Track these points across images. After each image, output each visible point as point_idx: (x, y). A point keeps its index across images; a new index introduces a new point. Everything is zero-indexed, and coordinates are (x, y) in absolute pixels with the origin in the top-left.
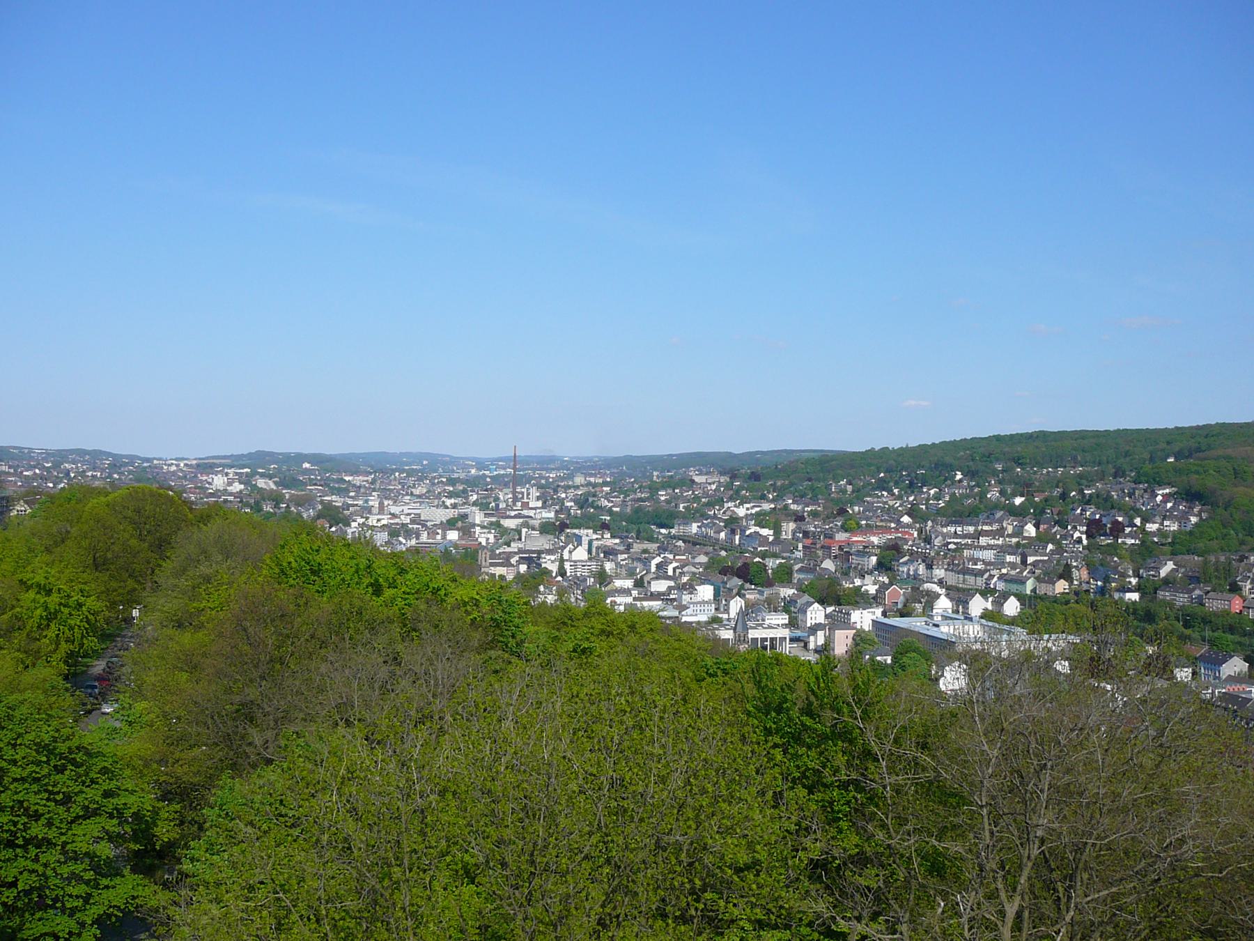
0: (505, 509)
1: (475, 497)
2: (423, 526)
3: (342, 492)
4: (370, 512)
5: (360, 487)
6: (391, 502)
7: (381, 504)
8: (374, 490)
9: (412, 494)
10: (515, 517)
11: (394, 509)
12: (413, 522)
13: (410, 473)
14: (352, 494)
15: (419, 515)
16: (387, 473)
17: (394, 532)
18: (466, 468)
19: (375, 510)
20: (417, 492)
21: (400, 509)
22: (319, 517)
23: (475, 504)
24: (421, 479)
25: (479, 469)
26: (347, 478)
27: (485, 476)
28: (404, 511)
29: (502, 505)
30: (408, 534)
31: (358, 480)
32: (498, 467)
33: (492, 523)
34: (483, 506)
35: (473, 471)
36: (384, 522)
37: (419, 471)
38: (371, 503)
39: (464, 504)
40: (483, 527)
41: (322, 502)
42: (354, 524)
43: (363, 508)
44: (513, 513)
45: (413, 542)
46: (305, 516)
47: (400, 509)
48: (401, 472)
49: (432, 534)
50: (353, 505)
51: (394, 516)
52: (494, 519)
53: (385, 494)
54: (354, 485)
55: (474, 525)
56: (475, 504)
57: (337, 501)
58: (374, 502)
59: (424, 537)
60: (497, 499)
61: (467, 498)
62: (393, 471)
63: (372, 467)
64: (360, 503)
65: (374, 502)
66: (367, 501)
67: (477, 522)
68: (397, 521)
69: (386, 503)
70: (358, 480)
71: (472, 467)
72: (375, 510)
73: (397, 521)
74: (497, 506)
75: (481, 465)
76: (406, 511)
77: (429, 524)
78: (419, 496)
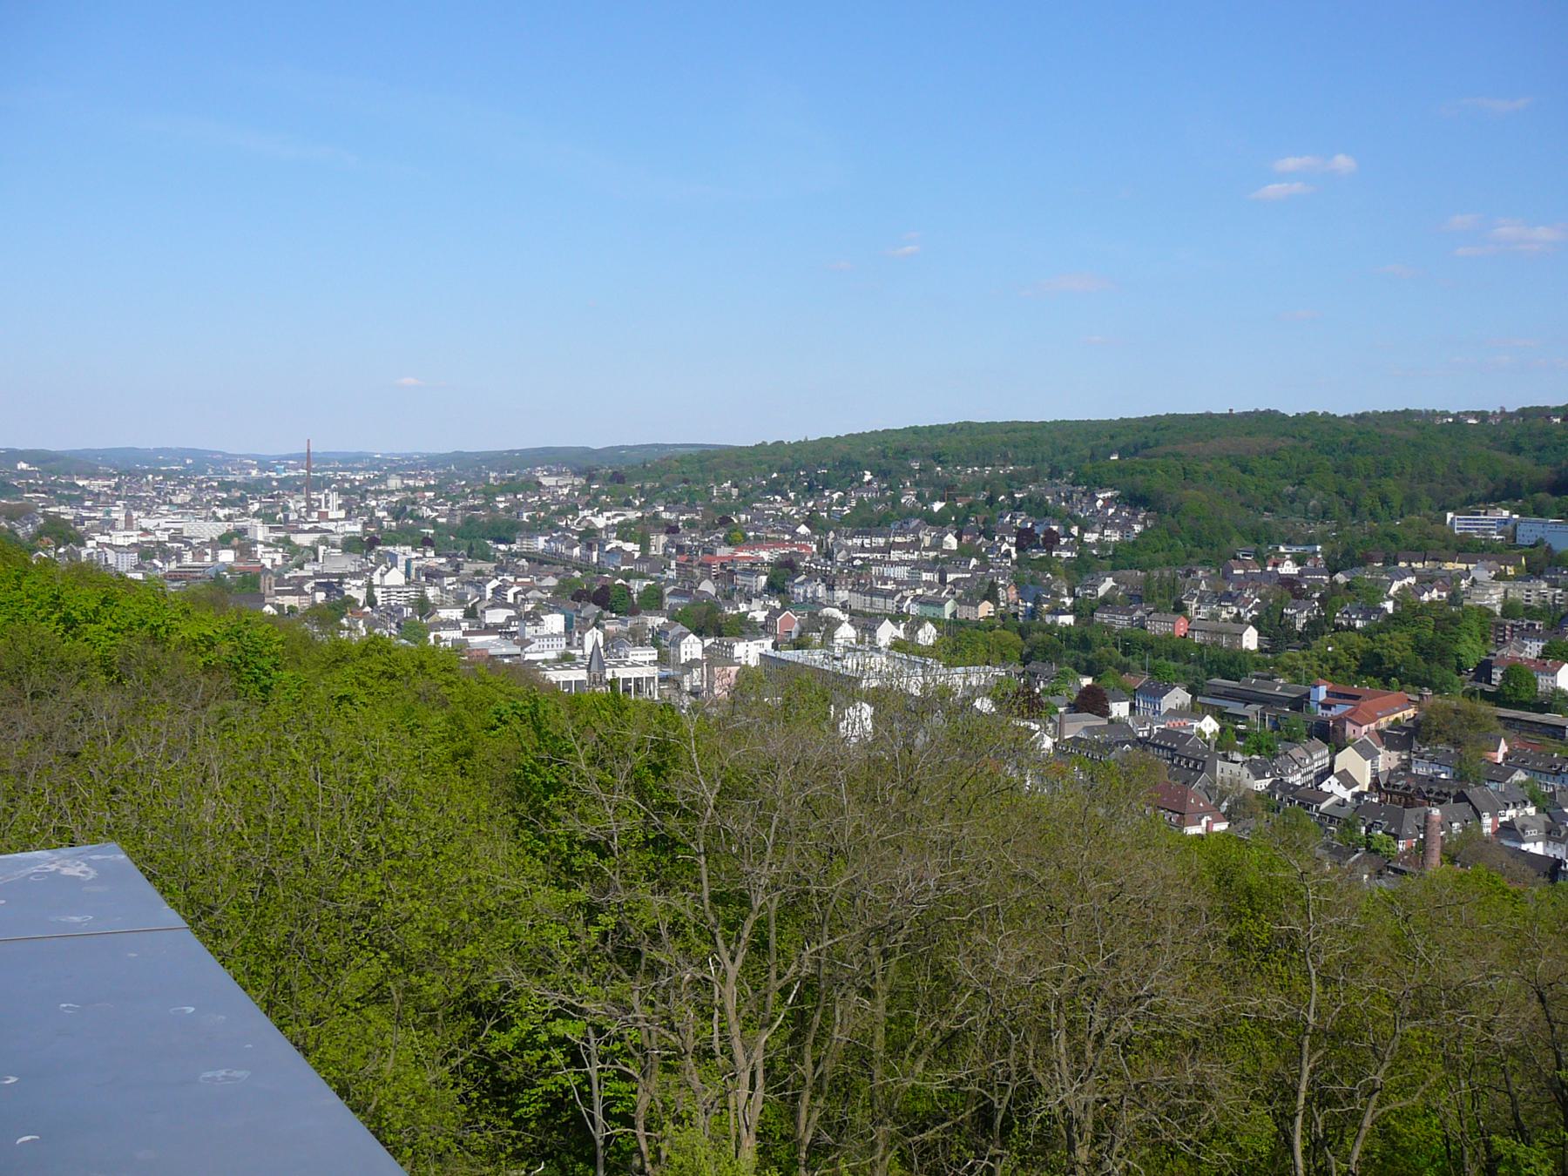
0: (297, 521)
1: (256, 506)
2: (187, 544)
3: (75, 500)
4: (113, 528)
5: (98, 494)
6: (142, 514)
7: (129, 518)
8: (119, 498)
9: (171, 503)
10: (310, 531)
11: (147, 523)
12: (173, 539)
13: (168, 476)
14: (88, 504)
15: (181, 530)
16: (138, 478)
17: (145, 553)
18: (244, 468)
19: (120, 525)
20: (178, 500)
21: (155, 522)
22: (41, 532)
23: (256, 515)
24: (183, 484)
25: (261, 470)
26: (81, 483)
27: (270, 479)
28: (160, 525)
29: (293, 517)
30: (166, 555)
31: (96, 485)
32: (288, 467)
33: (279, 540)
34: (266, 517)
36: (134, 540)
37: (181, 473)
38: (114, 516)
39: (243, 515)
40: (267, 545)
41: (45, 515)
42: (90, 543)
43: (102, 521)
44: (306, 527)
45: (173, 566)
46: (21, 533)
47: (155, 522)
48: (156, 474)
49: (199, 553)
50: (89, 519)
51: (146, 532)
52: (281, 535)
53: (134, 503)
54: (91, 492)
55: (255, 543)
56: (256, 515)
57: (67, 513)
58: (118, 514)
59: (188, 559)
60: (285, 508)
61: (245, 507)
62: (145, 473)
63: (116, 468)
64: (99, 515)
65: (118, 514)
66: (108, 513)
67: (260, 538)
68: (150, 538)
69: (135, 514)
70: (96, 485)
71: (253, 467)
72: (120, 525)
73: (150, 538)
74: (286, 517)
75: (264, 465)
76: (163, 526)
77: (194, 542)
78: (181, 506)
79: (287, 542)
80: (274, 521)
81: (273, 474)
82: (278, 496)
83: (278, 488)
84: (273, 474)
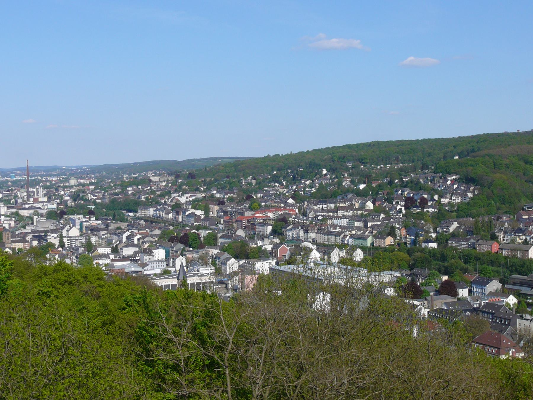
0: (22, 203)
27: (7, 181)
29: (20, 201)
32: (17, 175)
33: (12, 214)
40: (6, 216)
44: (27, 206)
52: (14, 211)
60: (16, 197)
67: (3, 213)
74: (16, 201)
79: (17, 214)
80: (10, 203)
81: (9, 179)
82: (12, 190)
84: (9, 179)
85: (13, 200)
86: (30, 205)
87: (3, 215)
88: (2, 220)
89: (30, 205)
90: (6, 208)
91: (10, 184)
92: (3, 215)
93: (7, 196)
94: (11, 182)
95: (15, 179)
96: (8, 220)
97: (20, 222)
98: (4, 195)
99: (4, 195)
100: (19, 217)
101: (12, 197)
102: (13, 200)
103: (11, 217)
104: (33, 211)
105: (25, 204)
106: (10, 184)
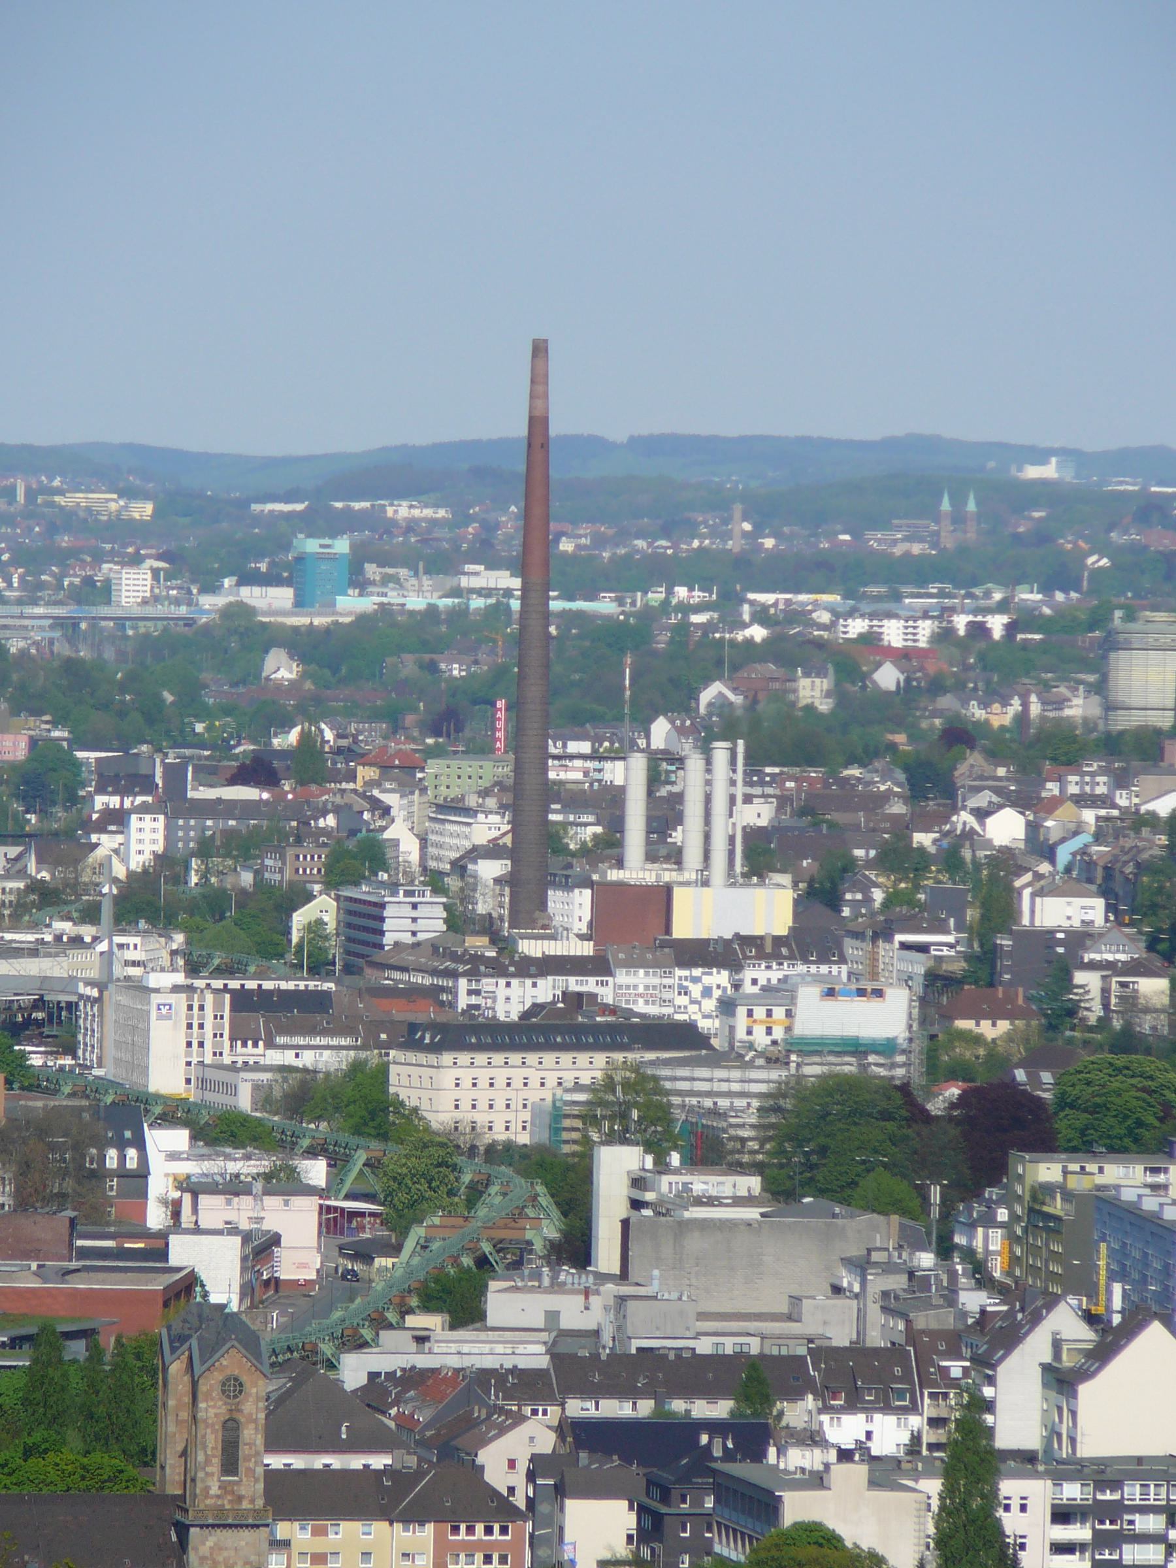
0: (445, 957)
1: (144, 839)
10: (536, 1032)
18: (61, 551)
23: (145, 902)
25: (188, 567)
27: (249, 635)
29: (412, 921)
32: (378, 550)
33: (302, 1096)
34: (218, 923)
35: (133, 587)
39: (45, 899)
40: (216, 1130)
44: (510, 999)
52: (323, 1055)
55: (131, 1112)
56: (145, 902)
60: (359, 859)
61: (67, 845)
67: (167, 1076)
71: (125, 542)
74: (364, 922)
75: (211, 525)
79: (364, 1108)
80: (271, 946)
81: (272, 601)
82: (309, 764)
83: (311, 707)
84: (272, 601)
85: (322, 910)
86: (545, 990)
87: (173, 1113)
88: (159, 1185)
89: (545, 990)
90: (215, 1012)
91: (282, 669)
92: (173, 1113)
93: (243, 847)
94: (301, 644)
95: (352, 604)
96: (234, 1188)
97: (400, 1220)
98: (190, 830)
99: (190, 830)
100: (393, 1154)
101: (309, 862)
102: (322, 910)
103: (284, 1144)
104: (587, 1068)
105: (477, 967)
106: (282, 669)
